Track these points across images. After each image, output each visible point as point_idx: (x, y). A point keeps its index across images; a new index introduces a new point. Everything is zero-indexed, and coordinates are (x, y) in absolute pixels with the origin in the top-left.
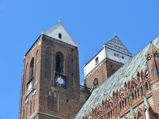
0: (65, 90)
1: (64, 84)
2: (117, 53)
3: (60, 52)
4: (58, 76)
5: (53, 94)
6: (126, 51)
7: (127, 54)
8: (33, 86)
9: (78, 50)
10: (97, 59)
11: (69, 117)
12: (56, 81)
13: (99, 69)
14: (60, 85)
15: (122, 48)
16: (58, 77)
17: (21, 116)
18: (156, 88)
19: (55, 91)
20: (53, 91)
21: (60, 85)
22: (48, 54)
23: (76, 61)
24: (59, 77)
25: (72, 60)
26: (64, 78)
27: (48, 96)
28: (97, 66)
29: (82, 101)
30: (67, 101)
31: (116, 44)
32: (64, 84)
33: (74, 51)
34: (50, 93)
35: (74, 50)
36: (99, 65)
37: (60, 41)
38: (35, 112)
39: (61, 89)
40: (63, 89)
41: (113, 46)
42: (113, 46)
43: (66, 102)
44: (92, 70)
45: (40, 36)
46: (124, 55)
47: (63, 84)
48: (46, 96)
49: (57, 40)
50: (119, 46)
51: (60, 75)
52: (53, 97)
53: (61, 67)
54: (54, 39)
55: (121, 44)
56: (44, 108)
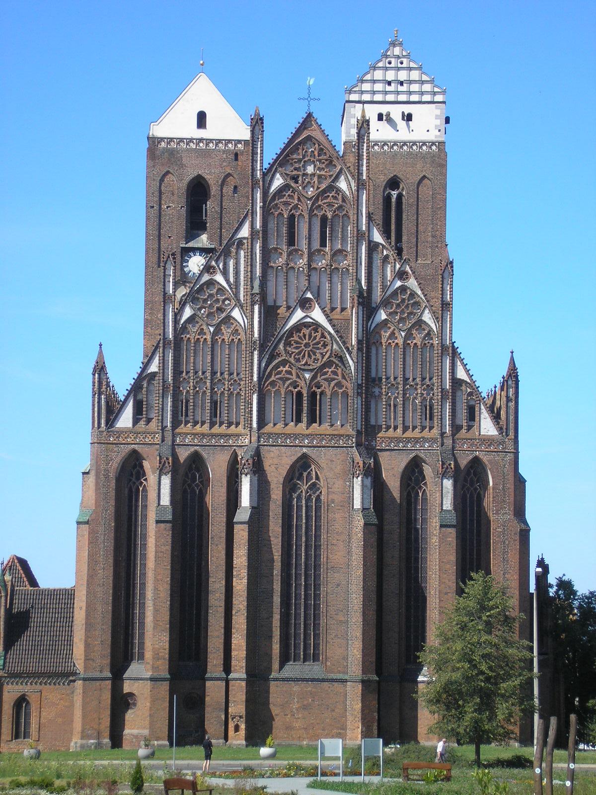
7: (427, 98)
12: (185, 269)
15: (410, 82)
16: (190, 257)
25: (235, 187)
31: (390, 75)
35: (242, 153)
37: (201, 140)
41: (379, 87)
42: (379, 87)
46: (407, 109)
50: (403, 75)
51: (194, 250)
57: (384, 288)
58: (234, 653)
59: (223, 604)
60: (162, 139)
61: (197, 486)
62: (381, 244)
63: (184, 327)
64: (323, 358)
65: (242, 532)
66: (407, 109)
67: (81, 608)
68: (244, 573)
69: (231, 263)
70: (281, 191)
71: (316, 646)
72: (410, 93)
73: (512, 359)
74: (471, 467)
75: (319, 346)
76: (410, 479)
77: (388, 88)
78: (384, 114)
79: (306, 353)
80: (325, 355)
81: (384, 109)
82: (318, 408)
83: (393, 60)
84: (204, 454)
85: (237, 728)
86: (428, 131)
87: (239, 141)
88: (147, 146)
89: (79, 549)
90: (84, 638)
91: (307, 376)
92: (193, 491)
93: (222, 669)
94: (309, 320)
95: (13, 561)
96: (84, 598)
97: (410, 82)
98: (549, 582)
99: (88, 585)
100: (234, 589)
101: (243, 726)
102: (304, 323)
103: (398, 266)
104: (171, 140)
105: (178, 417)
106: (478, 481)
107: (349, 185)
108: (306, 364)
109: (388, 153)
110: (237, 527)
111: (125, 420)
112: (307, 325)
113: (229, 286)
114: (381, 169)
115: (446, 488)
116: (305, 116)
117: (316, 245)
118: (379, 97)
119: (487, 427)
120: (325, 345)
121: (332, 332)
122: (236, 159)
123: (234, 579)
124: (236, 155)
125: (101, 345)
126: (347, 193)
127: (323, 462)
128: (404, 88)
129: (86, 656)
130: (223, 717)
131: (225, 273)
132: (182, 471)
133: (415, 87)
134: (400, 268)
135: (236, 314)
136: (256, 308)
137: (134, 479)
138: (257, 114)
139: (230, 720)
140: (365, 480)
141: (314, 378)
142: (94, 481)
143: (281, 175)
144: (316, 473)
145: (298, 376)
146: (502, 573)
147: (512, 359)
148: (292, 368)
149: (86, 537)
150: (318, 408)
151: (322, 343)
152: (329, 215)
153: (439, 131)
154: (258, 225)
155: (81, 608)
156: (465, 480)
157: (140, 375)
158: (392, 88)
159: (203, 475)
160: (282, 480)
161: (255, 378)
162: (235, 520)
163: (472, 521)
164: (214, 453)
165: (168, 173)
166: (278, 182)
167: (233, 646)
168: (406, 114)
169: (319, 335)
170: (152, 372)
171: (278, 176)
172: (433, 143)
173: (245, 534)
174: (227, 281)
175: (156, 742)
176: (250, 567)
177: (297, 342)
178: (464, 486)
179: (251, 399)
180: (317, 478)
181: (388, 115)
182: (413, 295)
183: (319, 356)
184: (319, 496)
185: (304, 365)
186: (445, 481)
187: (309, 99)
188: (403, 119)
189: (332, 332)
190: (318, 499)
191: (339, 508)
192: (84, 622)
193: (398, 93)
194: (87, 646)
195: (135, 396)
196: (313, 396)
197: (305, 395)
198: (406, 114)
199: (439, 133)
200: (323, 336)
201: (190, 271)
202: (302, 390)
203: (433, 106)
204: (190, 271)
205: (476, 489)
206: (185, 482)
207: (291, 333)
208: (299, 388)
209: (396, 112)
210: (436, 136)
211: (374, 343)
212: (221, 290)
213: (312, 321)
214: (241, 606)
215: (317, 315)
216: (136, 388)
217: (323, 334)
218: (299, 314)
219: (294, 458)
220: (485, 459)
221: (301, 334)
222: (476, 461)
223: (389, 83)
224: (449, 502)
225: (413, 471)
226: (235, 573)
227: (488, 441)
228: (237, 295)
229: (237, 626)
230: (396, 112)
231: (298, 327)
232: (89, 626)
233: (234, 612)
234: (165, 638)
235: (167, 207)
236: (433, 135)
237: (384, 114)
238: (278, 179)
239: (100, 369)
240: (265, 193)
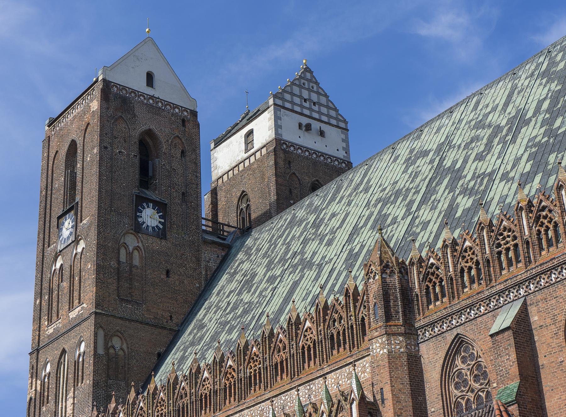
0: (164, 243)
1: (161, 227)
2: (305, 121)
3: (150, 130)
4: (145, 204)
5: (130, 255)
6: (333, 113)
8: (76, 227)
9: (200, 119)
10: (251, 132)
11: (171, 317)
12: (140, 220)
13: (256, 166)
14: (150, 229)
15: (320, 105)
16: (144, 208)
17: (41, 303)
18: (398, 347)
19: (137, 248)
20: (131, 248)
21: (150, 229)
22: (117, 141)
23: (193, 156)
24: (148, 207)
25: (183, 152)
26: (160, 207)
27: (119, 262)
28: (249, 158)
29: (206, 271)
30: (168, 272)
31: (305, 94)
32: (161, 227)
33: (189, 125)
34: (123, 252)
35: (189, 121)
36: (254, 154)
37: (152, 97)
38: (85, 305)
39: (151, 240)
40: (158, 241)
43: (163, 276)
44: (234, 165)
45: (96, 81)
47: (157, 226)
48: (114, 264)
49: (143, 94)
50: (314, 97)
51: (148, 200)
52: (131, 266)
53: (150, 174)
54: (134, 91)
55: (318, 93)
56: (109, 296)
60: (116, 85)
78: (304, 124)
81: (305, 121)
83: (306, 82)
87: (186, 110)
104: (124, 88)
122: (184, 125)
124: (183, 121)
128: (316, 108)
158: (307, 105)
201: (144, 223)
204: (144, 223)
209: (315, 125)
230: (315, 125)
235: (120, 152)
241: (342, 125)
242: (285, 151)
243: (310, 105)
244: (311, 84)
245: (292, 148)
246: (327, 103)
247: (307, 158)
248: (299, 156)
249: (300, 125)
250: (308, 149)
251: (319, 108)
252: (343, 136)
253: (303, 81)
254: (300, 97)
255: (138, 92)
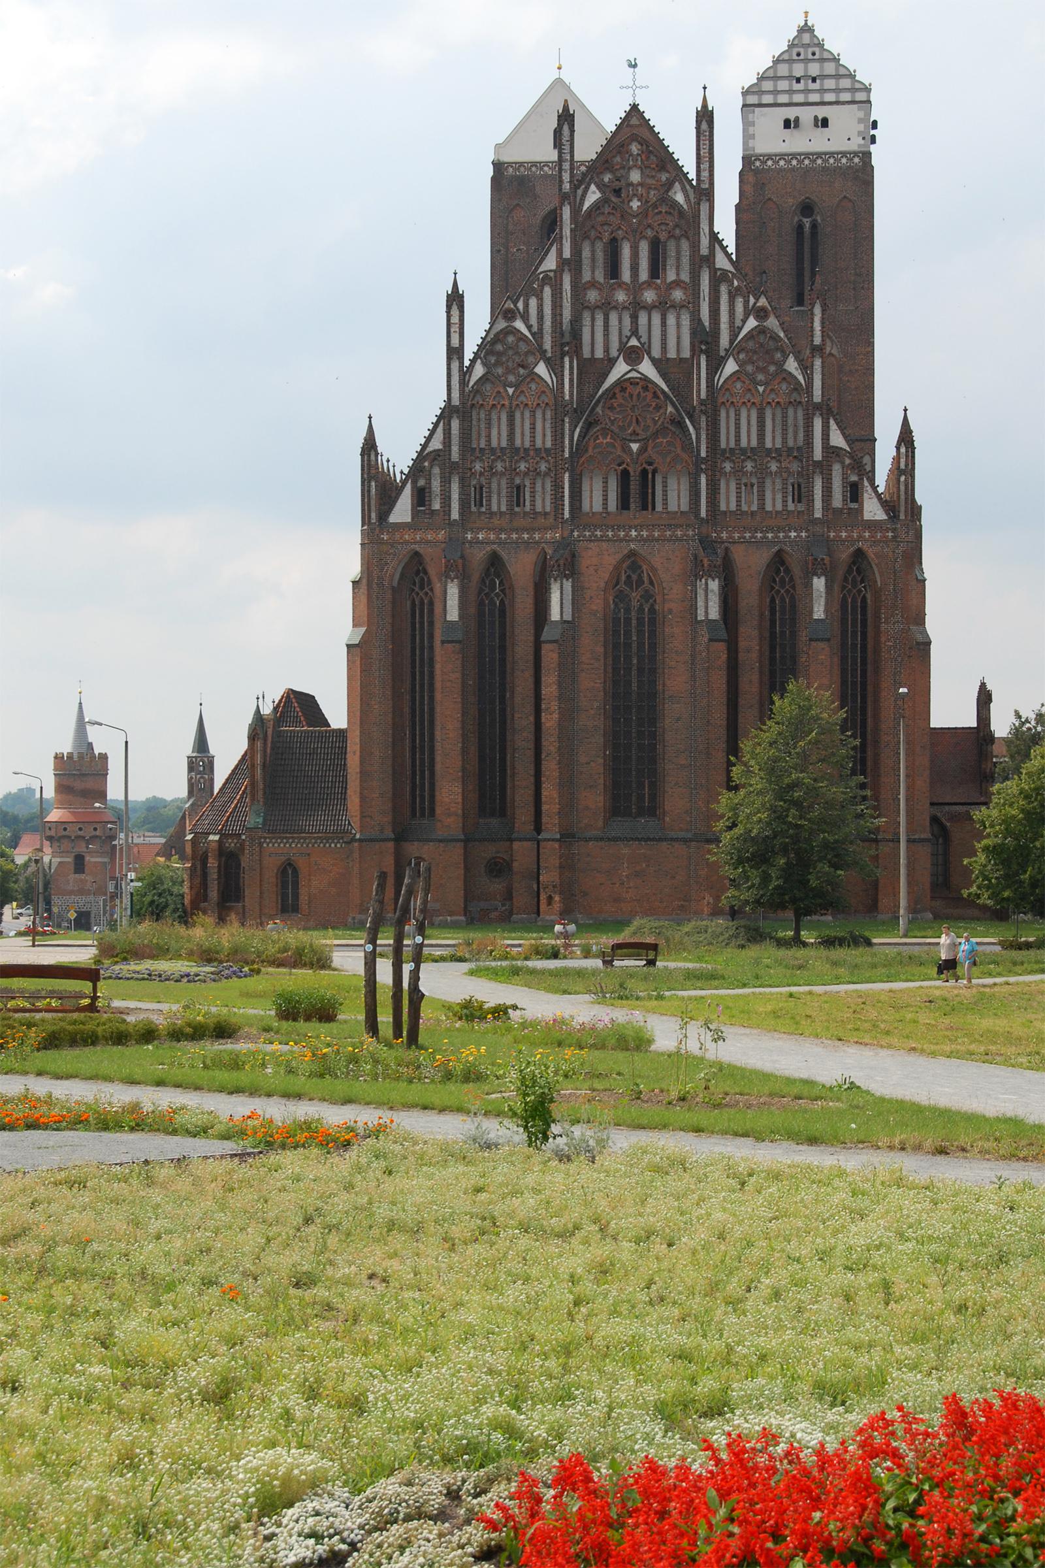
6: (845, 83)
15: (824, 77)
31: (798, 70)
41: (783, 85)
42: (783, 85)
50: (814, 69)
54: (534, 164)
57: (734, 331)
58: (544, 807)
59: (532, 746)
61: (497, 595)
62: (731, 272)
63: (476, 391)
64: (655, 425)
65: (551, 653)
66: (821, 112)
67: (354, 753)
68: (554, 705)
69: (533, 302)
70: (596, 206)
71: (653, 797)
72: (822, 91)
73: (905, 420)
74: (854, 563)
75: (651, 409)
76: (774, 581)
77: (796, 87)
78: (792, 120)
79: (634, 418)
80: (657, 421)
81: (791, 113)
82: (650, 491)
83: (802, 50)
84: (503, 554)
85: (550, 898)
86: (849, 139)
88: (491, 174)
89: (350, 678)
90: (358, 790)
91: (635, 447)
92: (492, 602)
93: (532, 828)
94: (634, 374)
95: (288, 696)
96: (358, 740)
97: (824, 77)
98: (96, 752)
99: (361, 723)
100: (543, 727)
101: (557, 898)
102: (630, 378)
103: (752, 300)
104: (521, 164)
105: (470, 507)
106: (862, 581)
107: (687, 196)
108: (634, 433)
109: (798, 169)
110: (545, 648)
111: (402, 511)
112: (632, 382)
113: (532, 334)
114: (789, 190)
115: (818, 590)
116: (628, 108)
117: (644, 276)
118: (783, 99)
119: (873, 510)
120: (658, 408)
121: (666, 389)
123: (543, 714)
125: (370, 418)
126: (685, 207)
127: (657, 561)
128: (816, 86)
129: (362, 812)
130: (535, 886)
131: (525, 318)
132: (476, 577)
133: (830, 84)
134: (755, 304)
135: (541, 369)
136: (567, 359)
137: (417, 589)
138: (566, 108)
139: (542, 890)
140: (710, 582)
141: (643, 450)
142: (366, 592)
143: (598, 187)
144: (649, 575)
145: (624, 450)
146: (893, 699)
147: (906, 422)
148: (615, 440)
149: (358, 662)
150: (650, 491)
151: (654, 404)
152: (663, 236)
153: (864, 138)
154: (567, 254)
155: (354, 753)
156: (845, 579)
157: (420, 453)
158: (800, 86)
159: (504, 581)
160: (602, 585)
161: (567, 455)
162: (542, 639)
163: (854, 633)
164: (516, 553)
165: (518, 205)
166: (593, 195)
167: (544, 799)
168: (820, 118)
169: (650, 395)
170: (435, 451)
171: (593, 187)
172: (856, 154)
173: (555, 656)
174: (529, 327)
175: (449, 918)
176: (561, 698)
177: (620, 405)
178: (844, 587)
179: (563, 482)
180: (651, 583)
181: (797, 119)
182: (775, 338)
183: (649, 422)
184: (652, 605)
185: (631, 435)
186: (815, 580)
187: (634, 87)
188: (816, 125)
189: (666, 389)
190: (652, 610)
191: (679, 620)
192: (358, 770)
193: (807, 91)
194: (363, 798)
195: (414, 483)
196: (644, 473)
197: (632, 474)
198: (820, 118)
199: (862, 142)
200: (655, 395)
202: (628, 468)
203: (855, 106)
205: (860, 591)
206: (481, 591)
207: (611, 392)
208: (624, 466)
209: (806, 115)
210: (859, 146)
211: (723, 403)
212: (523, 338)
213: (639, 376)
214: (552, 748)
215: (647, 368)
216: (418, 468)
217: (655, 392)
218: (621, 369)
219: (619, 557)
220: (871, 552)
221: (627, 395)
222: (859, 554)
223: (798, 80)
224: (822, 609)
225: (778, 571)
226: (543, 706)
227: (873, 525)
228: (540, 345)
229: (548, 773)
230: (806, 115)
231: (621, 383)
232: (364, 775)
233: (543, 757)
234: (457, 789)
236: (855, 144)
237: (792, 120)
238: (594, 193)
239: (370, 447)
240: (575, 212)
241: (860, 96)
242: (757, 172)
243: (806, 84)
244: (810, 50)
245: (770, 163)
246: (837, 69)
247: (793, 169)
248: (781, 170)
249: (787, 124)
250: (794, 156)
251: (822, 84)
252: (861, 114)
253: (795, 51)
254: (789, 77)
255: (540, 163)
